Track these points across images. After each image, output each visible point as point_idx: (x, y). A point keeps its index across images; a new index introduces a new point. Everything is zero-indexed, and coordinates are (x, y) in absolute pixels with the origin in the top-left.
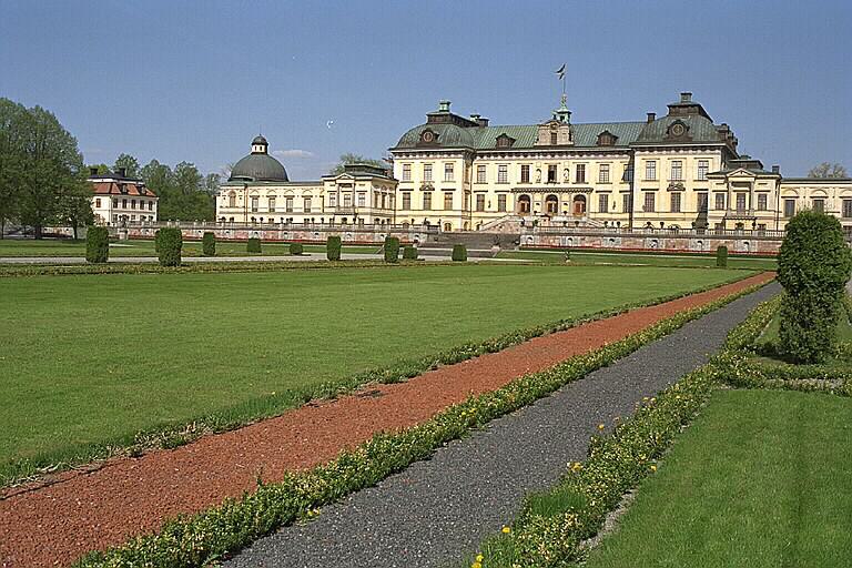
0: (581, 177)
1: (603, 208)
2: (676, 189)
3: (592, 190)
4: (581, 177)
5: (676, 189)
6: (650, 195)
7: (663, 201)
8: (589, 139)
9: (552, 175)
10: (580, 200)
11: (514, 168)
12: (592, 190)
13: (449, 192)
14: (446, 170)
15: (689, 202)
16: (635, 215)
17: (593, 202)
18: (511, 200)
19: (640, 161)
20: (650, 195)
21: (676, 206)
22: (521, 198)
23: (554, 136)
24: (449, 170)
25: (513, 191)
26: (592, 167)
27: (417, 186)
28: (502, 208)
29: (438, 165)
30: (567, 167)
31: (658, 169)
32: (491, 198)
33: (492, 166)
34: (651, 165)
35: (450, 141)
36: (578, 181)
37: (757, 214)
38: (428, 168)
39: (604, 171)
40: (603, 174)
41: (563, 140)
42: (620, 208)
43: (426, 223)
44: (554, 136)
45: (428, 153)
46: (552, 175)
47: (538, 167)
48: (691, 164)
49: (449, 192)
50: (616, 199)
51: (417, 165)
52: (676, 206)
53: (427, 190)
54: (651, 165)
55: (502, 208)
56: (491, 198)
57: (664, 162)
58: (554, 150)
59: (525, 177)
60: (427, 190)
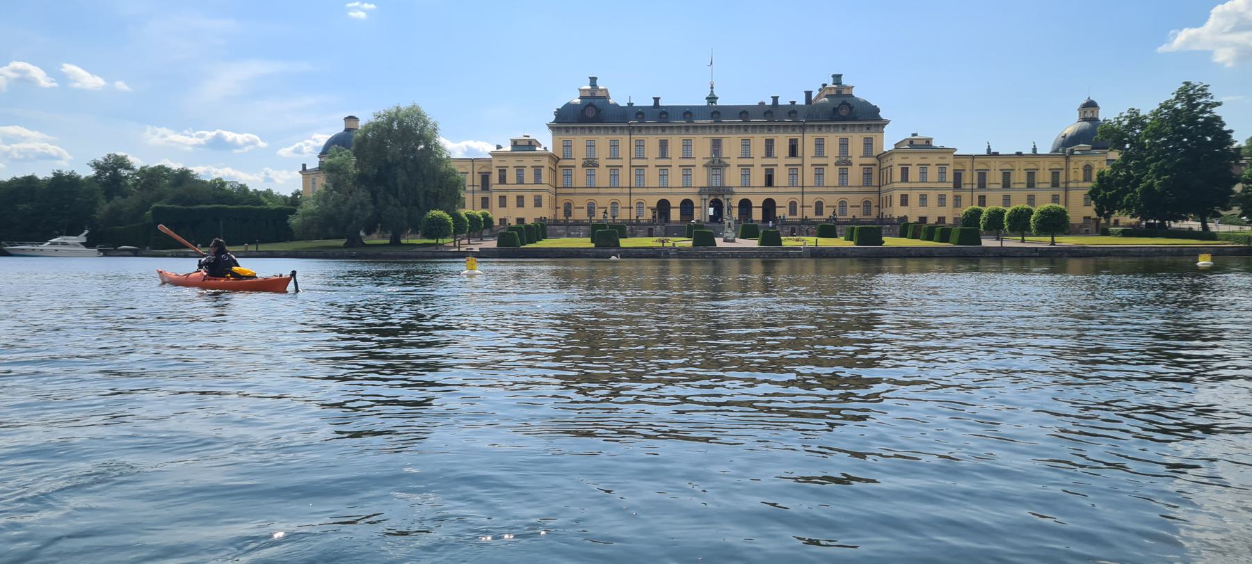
2: (844, 163)
5: (844, 163)
7: (831, 176)
13: (615, 170)
15: (855, 175)
27: (579, 162)
29: (603, 141)
38: (591, 145)
45: (591, 129)
48: (856, 140)
51: (579, 142)
53: (590, 164)
57: (832, 140)
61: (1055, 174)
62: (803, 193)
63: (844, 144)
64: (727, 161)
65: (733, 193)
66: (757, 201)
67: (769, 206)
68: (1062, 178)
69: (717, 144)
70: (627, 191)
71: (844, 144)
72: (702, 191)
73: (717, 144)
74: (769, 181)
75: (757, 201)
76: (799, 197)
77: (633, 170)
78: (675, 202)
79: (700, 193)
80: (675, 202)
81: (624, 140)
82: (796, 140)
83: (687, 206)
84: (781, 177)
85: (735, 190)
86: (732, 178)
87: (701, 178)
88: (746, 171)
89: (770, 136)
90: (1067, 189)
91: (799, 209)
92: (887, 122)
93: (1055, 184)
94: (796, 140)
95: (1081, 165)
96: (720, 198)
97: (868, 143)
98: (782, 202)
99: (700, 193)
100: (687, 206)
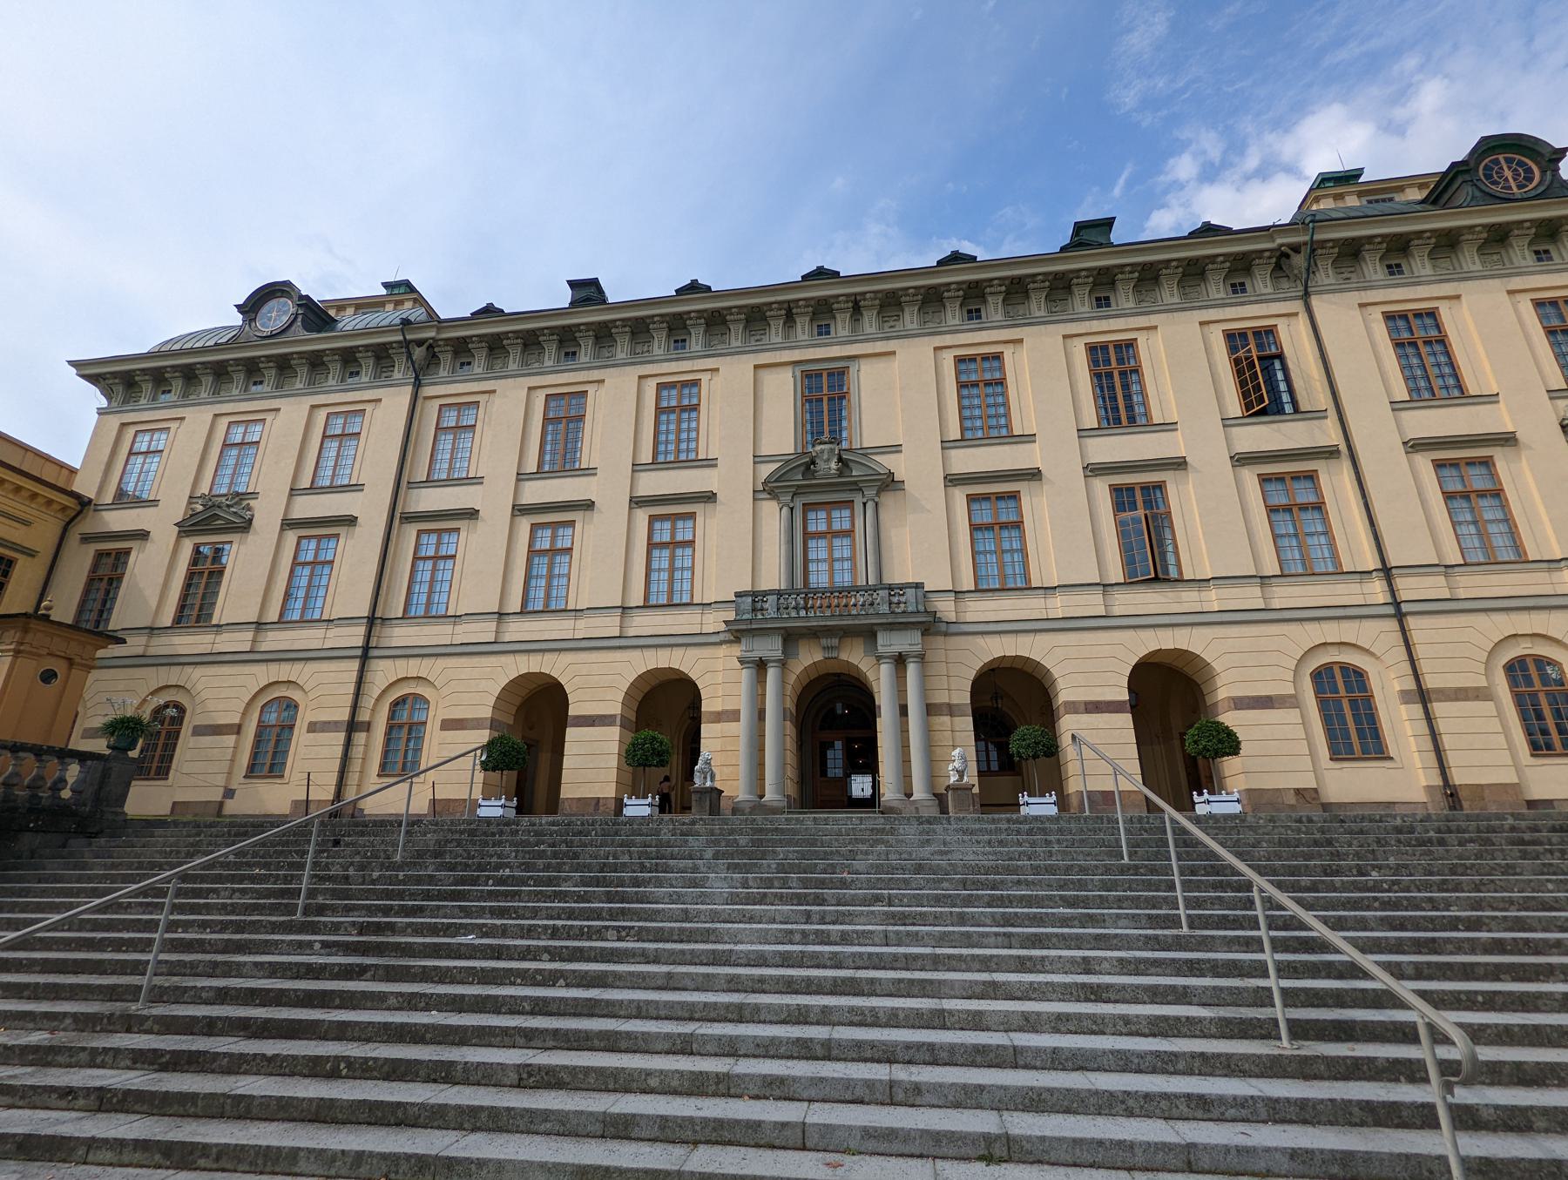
62: (1398, 611)
64: (887, 462)
65: (931, 626)
66: (1089, 675)
67: (1171, 703)
69: (825, 396)
70: (354, 636)
72: (751, 619)
73: (825, 396)
74: (1149, 551)
75: (1089, 675)
76: (1380, 635)
77: (408, 535)
78: (599, 687)
79: (736, 633)
80: (599, 687)
82: (1266, 334)
83: (665, 716)
84: (1216, 522)
85: (946, 608)
86: (921, 544)
87: (741, 549)
88: (995, 506)
89: (1110, 328)
91: (1399, 723)
94: (1266, 334)
96: (855, 656)
98: (1246, 668)
99: (736, 633)
100: (665, 716)
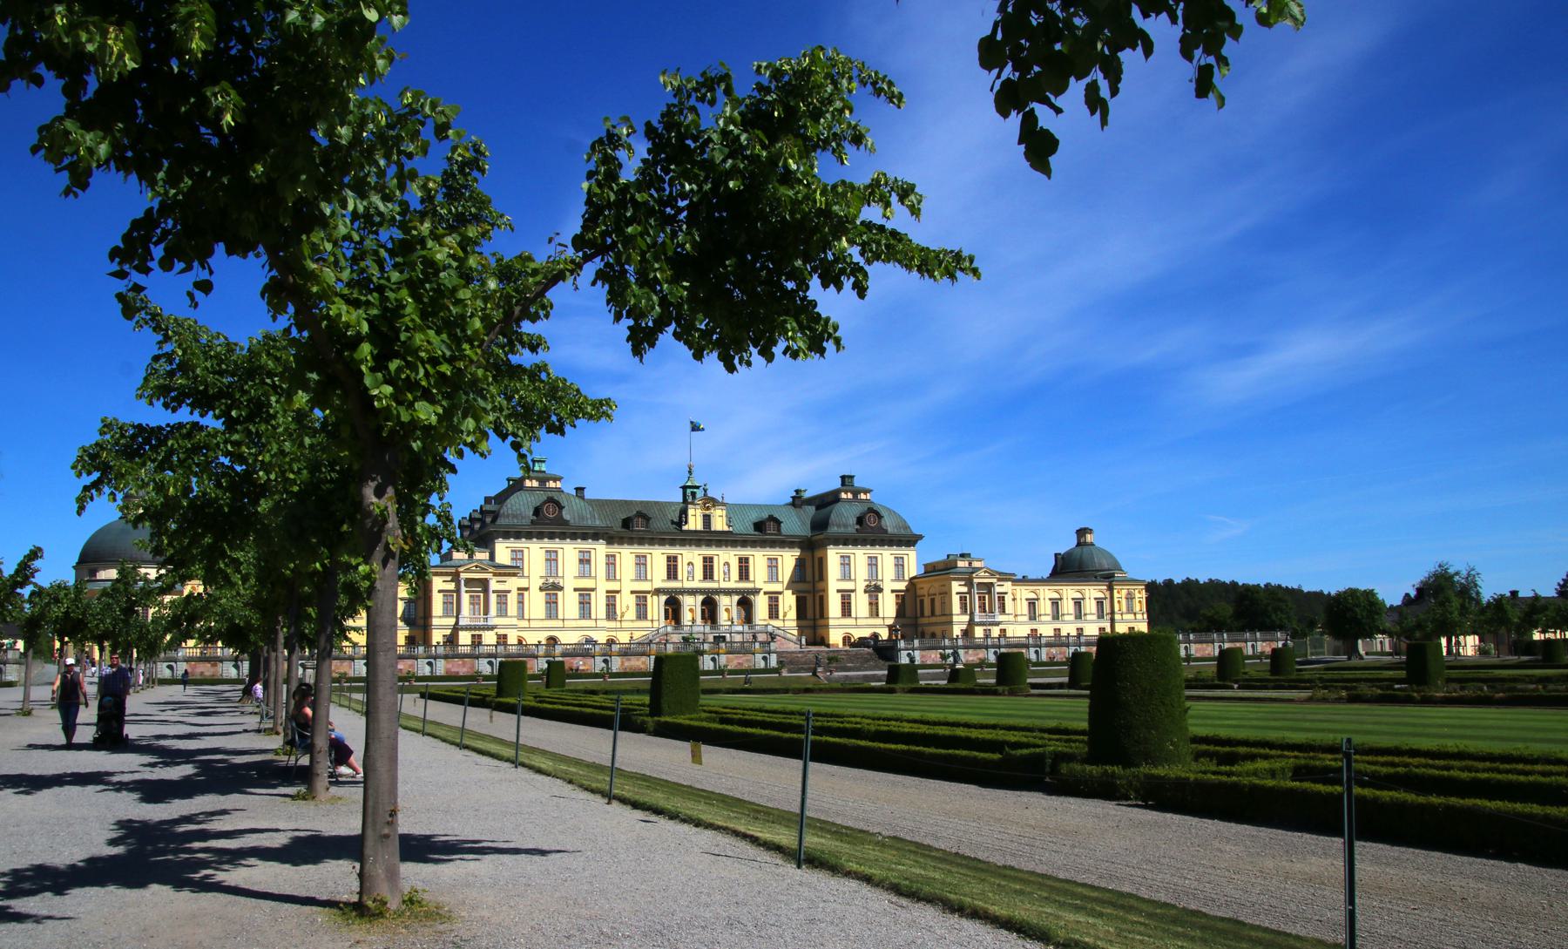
0: (744, 574)
1: (774, 612)
2: (874, 590)
3: (756, 591)
4: (744, 574)
5: (874, 590)
6: (846, 598)
7: (861, 603)
8: (745, 527)
9: (708, 573)
10: (746, 604)
11: (657, 557)
12: (756, 591)
14: (581, 561)
15: (888, 606)
16: (831, 622)
17: (761, 605)
18: (656, 606)
19: (833, 555)
20: (846, 598)
21: (874, 610)
22: (667, 603)
23: (707, 519)
24: (585, 561)
25: (658, 592)
26: (759, 559)
27: (536, 582)
28: (642, 614)
29: (569, 551)
30: (727, 558)
31: (848, 568)
32: (627, 603)
33: (626, 555)
34: (846, 562)
35: (582, 518)
36: (741, 578)
37: (1000, 618)
39: (773, 565)
40: (771, 569)
41: (719, 523)
42: (793, 614)
43: (553, 641)
44: (707, 519)
45: (552, 536)
46: (708, 573)
47: (691, 556)
48: (886, 556)
49: (585, 596)
50: (788, 602)
52: (874, 610)
54: (846, 562)
55: (642, 614)
56: (627, 603)
57: (860, 555)
58: (707, 537)
59: (672, 573)
60: (552, 589)
61: (1100, 603)
63: (873, 563)
68: (1107, 608)
71: (873, 563)
81: (600, 550)
90: (1113, 621)
92: (920, 537)
93: (1101, 616)
95: (1124, 592)
97: (899, 564)
